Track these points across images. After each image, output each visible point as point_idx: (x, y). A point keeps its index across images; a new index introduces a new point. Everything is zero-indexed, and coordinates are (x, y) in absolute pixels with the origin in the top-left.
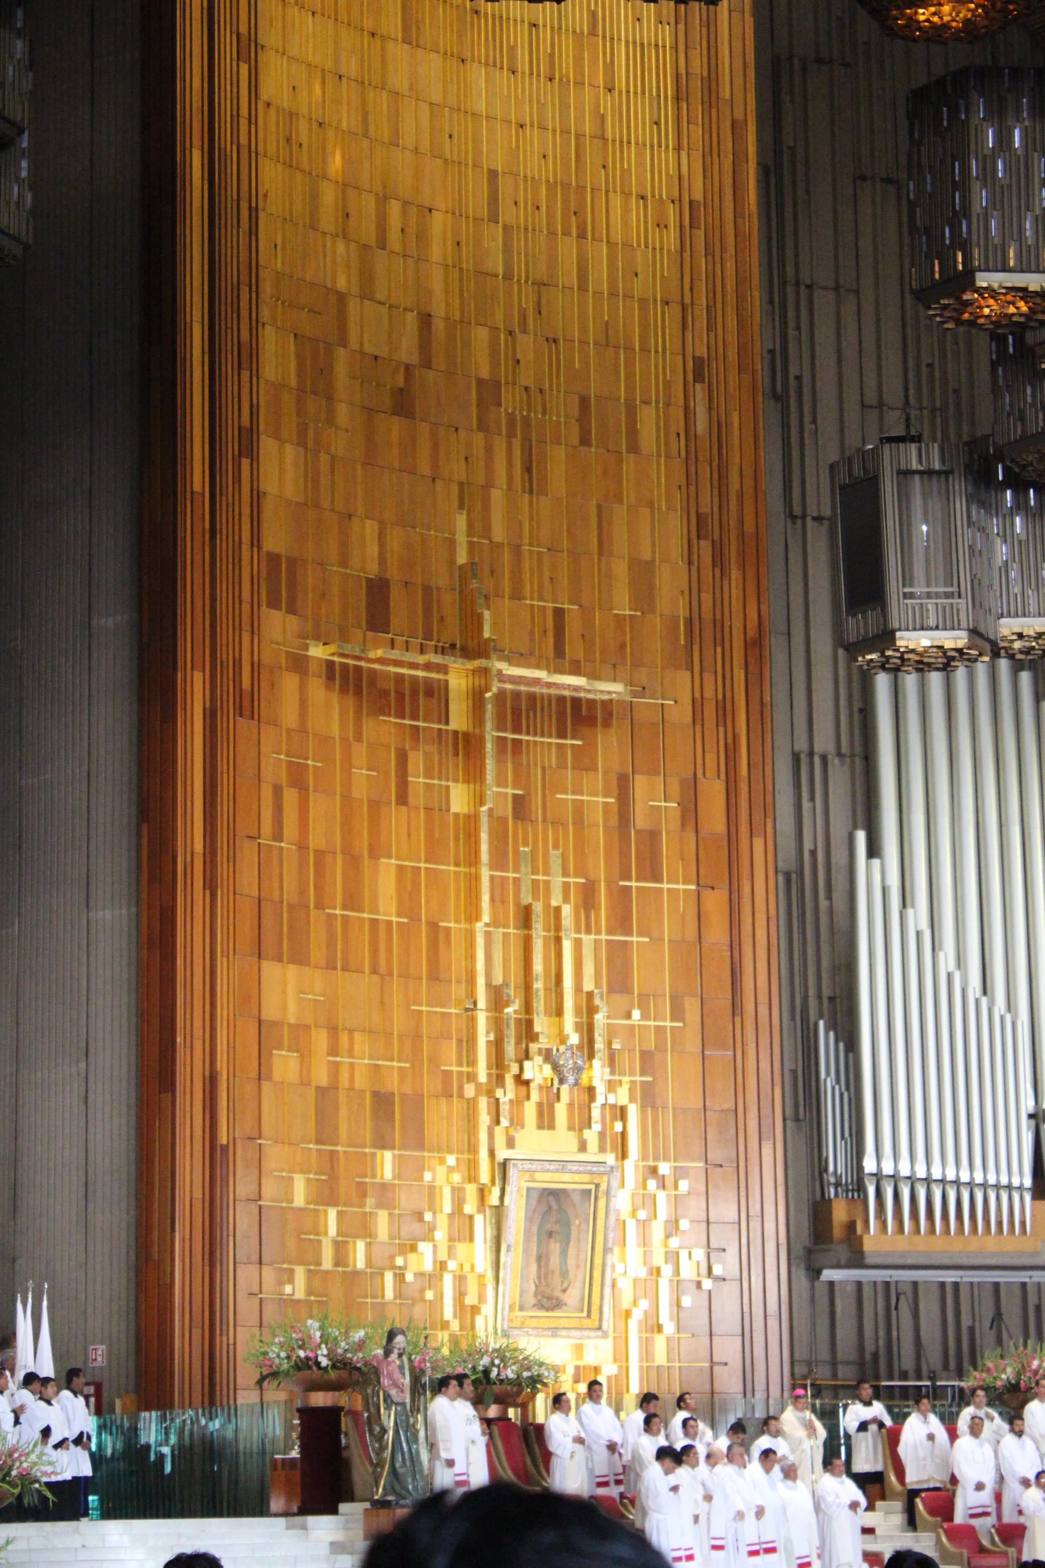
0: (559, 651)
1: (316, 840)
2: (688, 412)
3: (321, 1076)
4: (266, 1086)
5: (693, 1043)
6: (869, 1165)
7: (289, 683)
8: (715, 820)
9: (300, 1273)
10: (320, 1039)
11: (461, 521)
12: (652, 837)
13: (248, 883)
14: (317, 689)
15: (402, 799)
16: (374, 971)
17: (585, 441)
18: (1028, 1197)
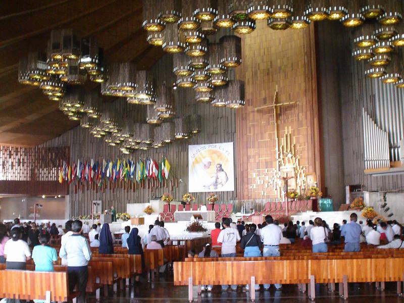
0: (290, 99)
1: (256, 132)
2: (305, 60)
3: (257, 161)
4: (249, 164)
5: (306, 149)
6: (365, 159)
7: (251, 115)
8: (309, 117)
9: (255, 185)
10: (257, 157)
11: (277, 86)
12: (301, 121)
13: (245, 139)
14: (256, 114)
15: (269, 124)
16: (265, 147)
17: (292, 70)
18: (389, 161)
